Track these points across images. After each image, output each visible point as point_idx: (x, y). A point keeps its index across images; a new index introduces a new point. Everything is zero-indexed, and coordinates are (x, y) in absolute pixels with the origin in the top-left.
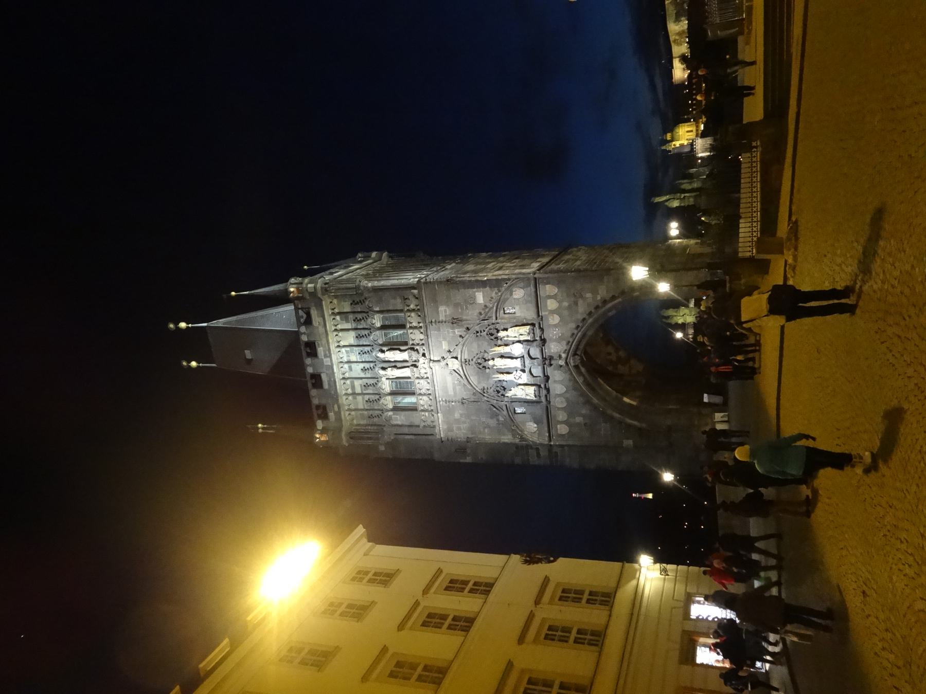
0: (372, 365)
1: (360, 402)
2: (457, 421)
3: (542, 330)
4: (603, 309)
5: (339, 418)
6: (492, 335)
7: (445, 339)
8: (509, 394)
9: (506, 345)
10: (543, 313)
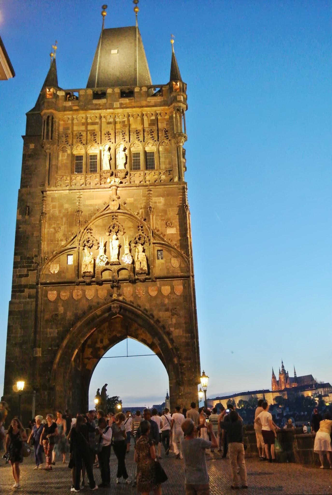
2: (61, 206)
3: (144, 281)
5: (65, 109)
6: (139, 239)
7: (135, 200)
9: (130, 250)
10: (158, 283)
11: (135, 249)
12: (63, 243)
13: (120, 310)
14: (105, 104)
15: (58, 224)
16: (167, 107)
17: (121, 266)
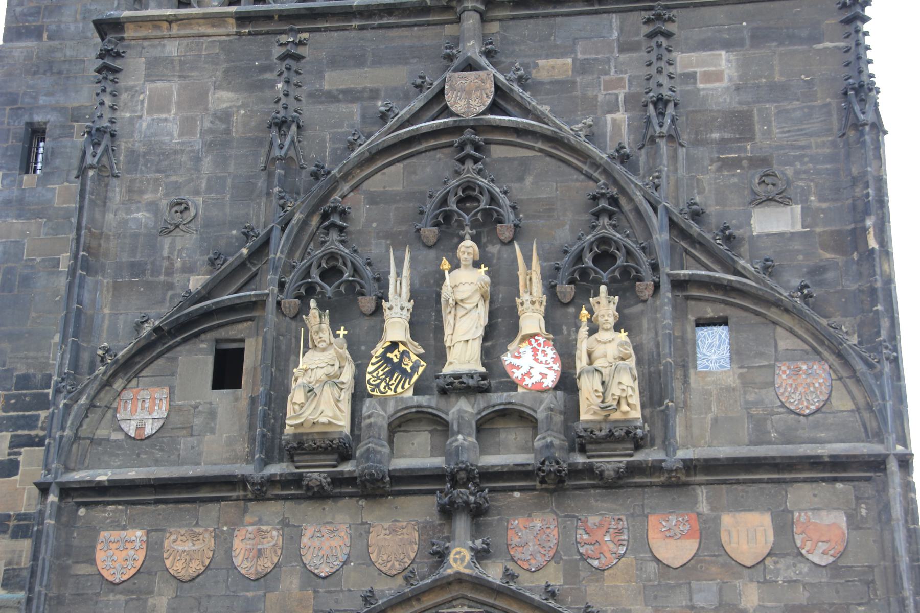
11: (577, 315)
12: (196, 282)
15: (177, 187)
17: (498, 398)
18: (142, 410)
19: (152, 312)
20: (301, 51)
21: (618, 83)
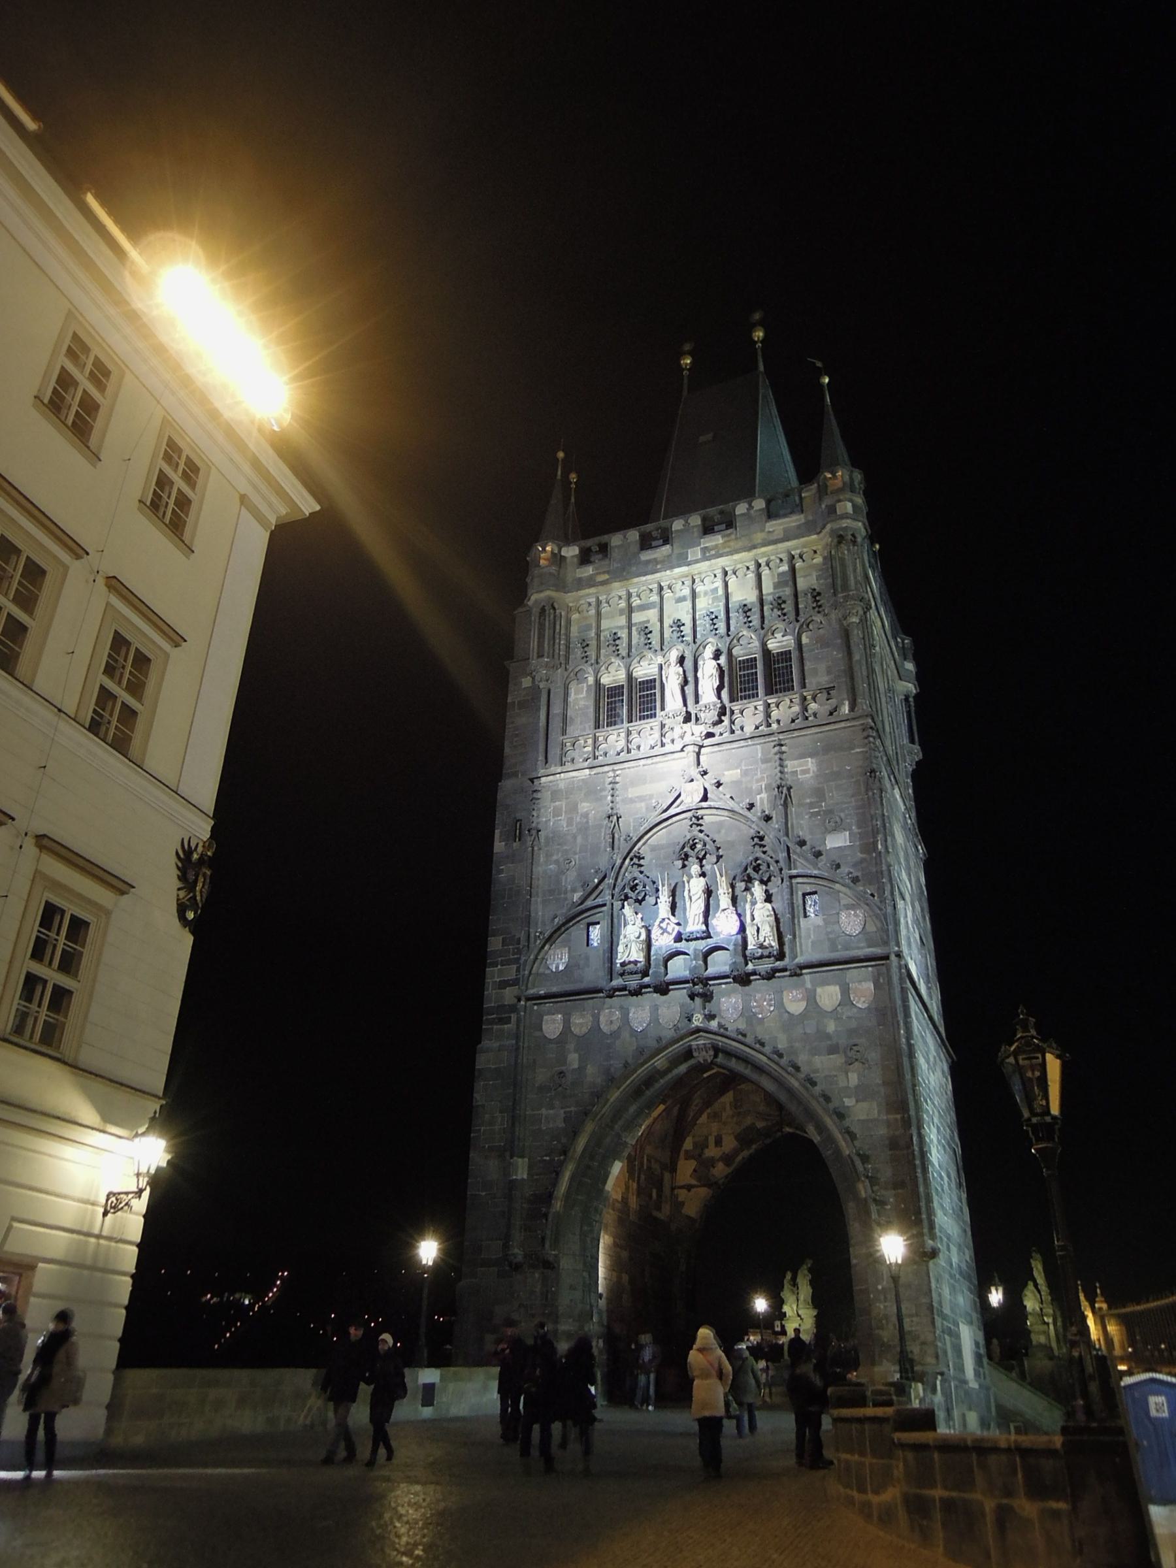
0: (689, 638)
1: (613, 623)
2: (573, 808)
3: (770, 976)
4: (820, 1111)
5: (581, 584)
7: (745, 773)
8: (628, 910)
9: (734, 900)
10: (808, 978)
12: (576, 897)
13: (716, 1056)
14: (669, 556)
16: (814, 537)
18: (558, 960)
19: (559, 913)
20: (618, 779)
21: (762, 779)
